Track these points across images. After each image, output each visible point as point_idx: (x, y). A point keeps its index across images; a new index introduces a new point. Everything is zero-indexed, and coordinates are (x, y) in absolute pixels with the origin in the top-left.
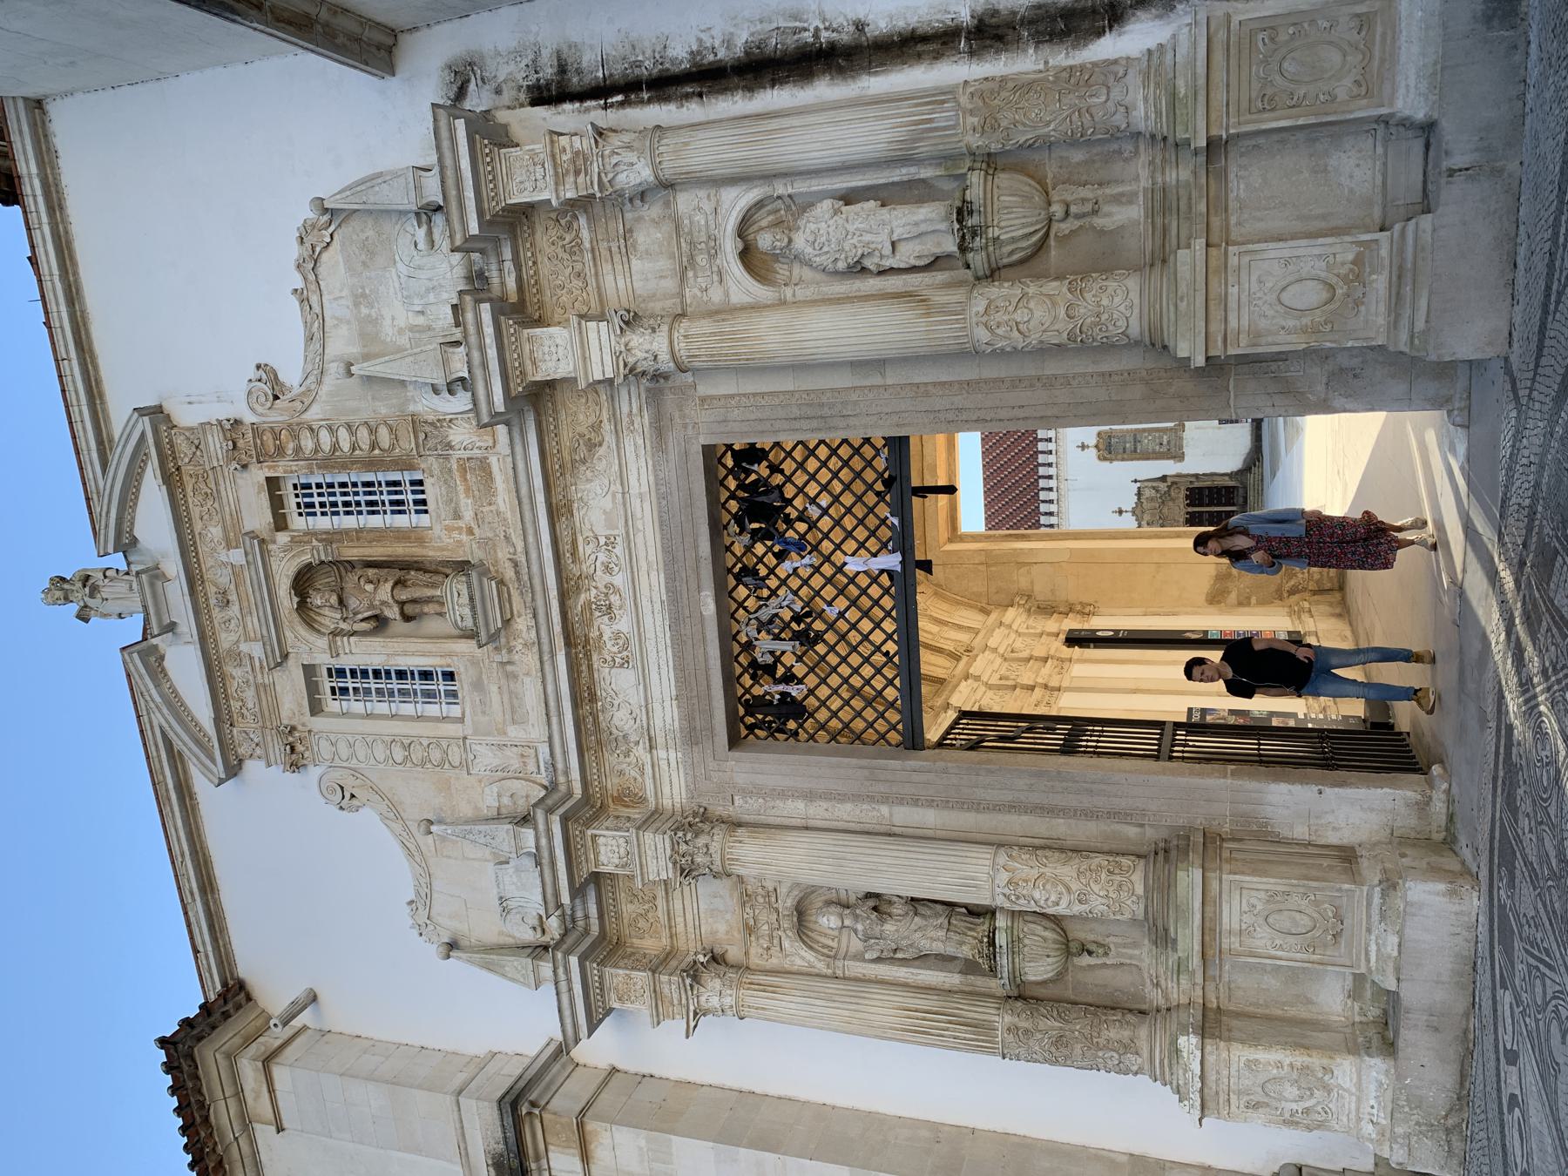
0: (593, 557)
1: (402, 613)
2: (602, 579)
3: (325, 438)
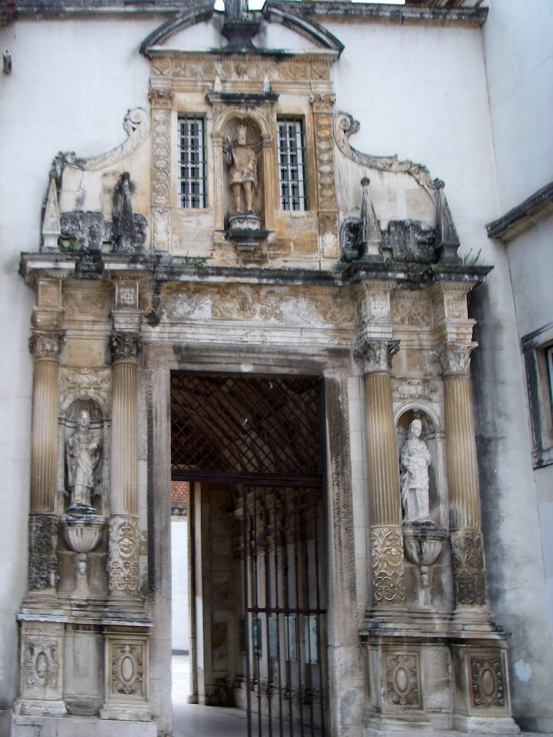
0: (270, 305)
1: (237, 183)
2: (258, 307)
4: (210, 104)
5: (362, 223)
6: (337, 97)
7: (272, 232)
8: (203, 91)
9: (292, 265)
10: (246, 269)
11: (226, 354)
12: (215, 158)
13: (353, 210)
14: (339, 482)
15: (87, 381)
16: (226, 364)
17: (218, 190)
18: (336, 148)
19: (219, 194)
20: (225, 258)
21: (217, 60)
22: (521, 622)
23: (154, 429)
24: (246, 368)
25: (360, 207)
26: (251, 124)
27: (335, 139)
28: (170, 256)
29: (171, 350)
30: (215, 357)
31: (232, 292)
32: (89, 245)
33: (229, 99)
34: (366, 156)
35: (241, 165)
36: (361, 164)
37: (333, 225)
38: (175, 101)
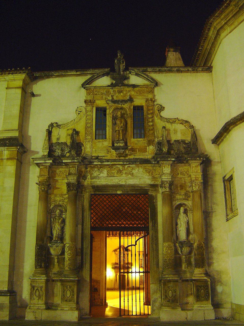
3: (151, 120)
11: (112, 188)
14: (153, 229)
15: (59, 199)
16: (112, 191)
17: (110, 133)
19: (110, 134)
22: (219, 273)
23: (84, 214)
24: (119, 192)
29: (91, 187)
30: (108, 189)
31: (114, 167)
32: (61, 154)
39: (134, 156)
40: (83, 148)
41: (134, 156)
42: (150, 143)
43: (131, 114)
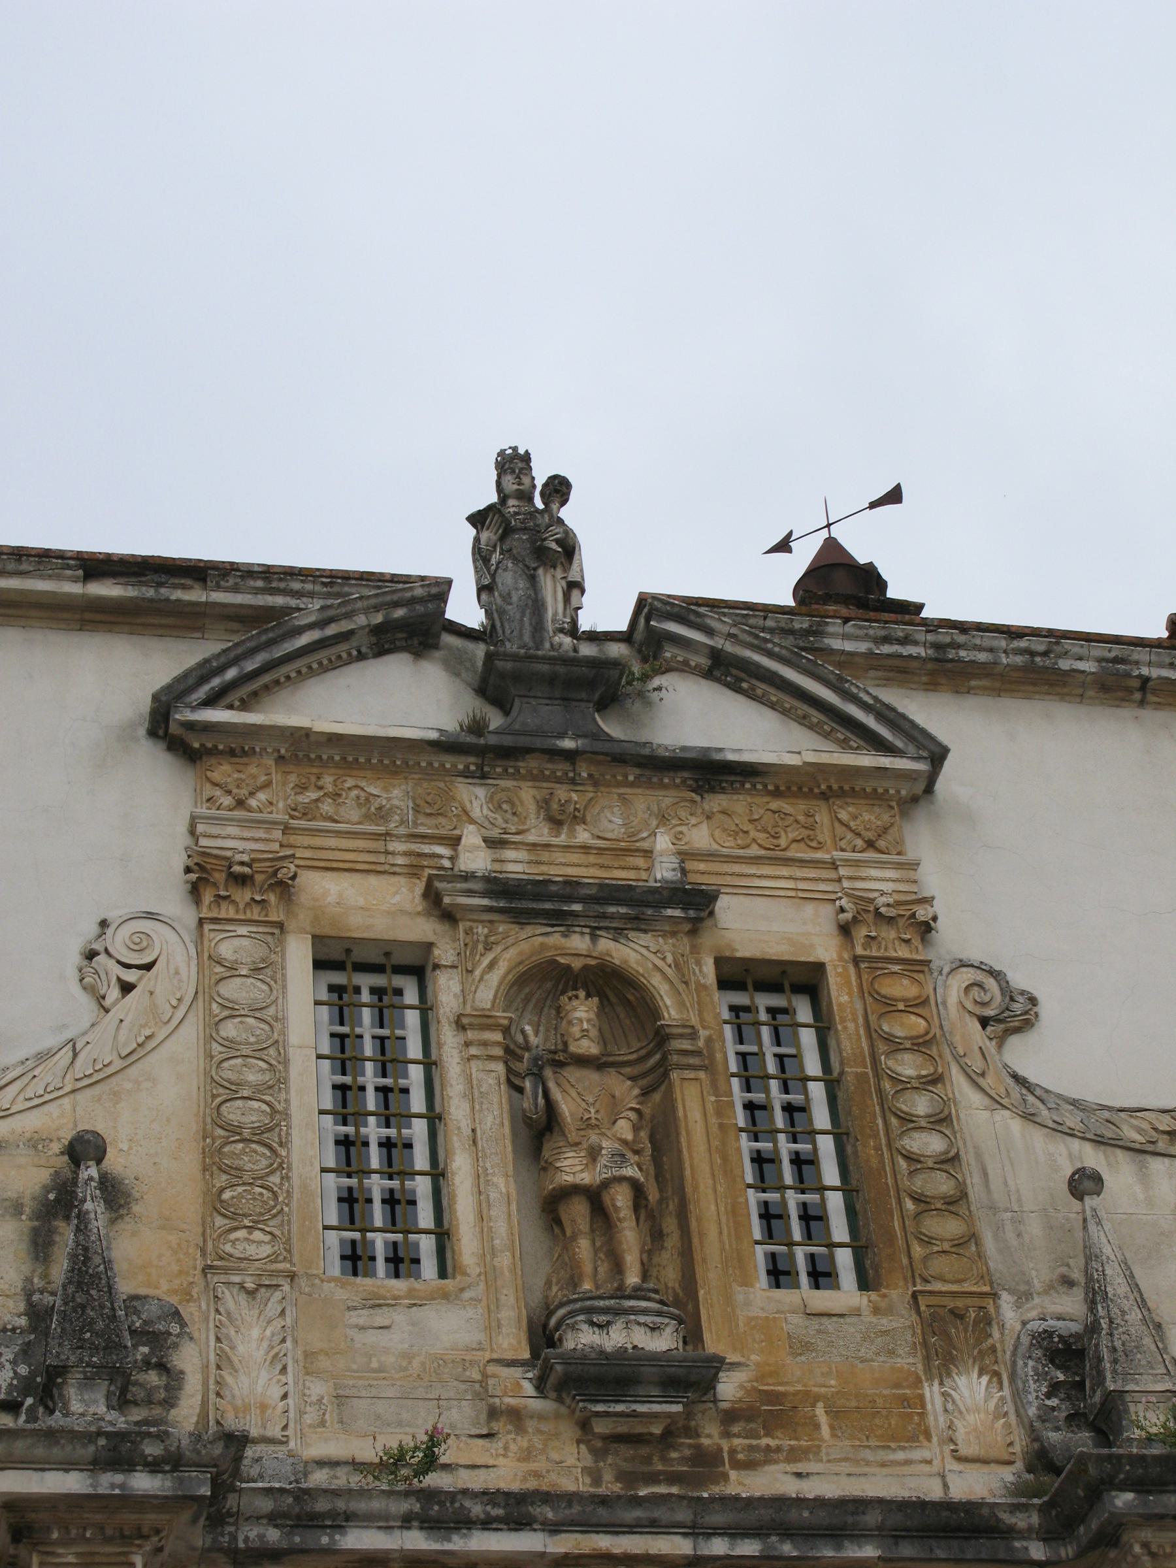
1: (575, 1190)
4: (449, 916)
5: (1093, 1328)
6: (939, 907)
7: (734, 1366)
8: (413, 871)
9: (827, 1484)
10: (637, 1501)
12: (474, 1103)
13: (1049, 1288)
18: (956, 1076)
19: (501, 1228)
20: (539, 1465)
21: (466, 774)
25: (1077, 1275)
26: (612, 987)
27: (951, 1045)
28: (291, 1454)
33: (518, 900)
34: (1074, 1103)
35: (587, 1125)
36: (1059, 1130)
37: (979, 1342)
38: (304, 899)
39: (799, 1475)
40: (188, 1359)
41: (799, 1475)
42: (951, 1330)
43: (703, 1033)
